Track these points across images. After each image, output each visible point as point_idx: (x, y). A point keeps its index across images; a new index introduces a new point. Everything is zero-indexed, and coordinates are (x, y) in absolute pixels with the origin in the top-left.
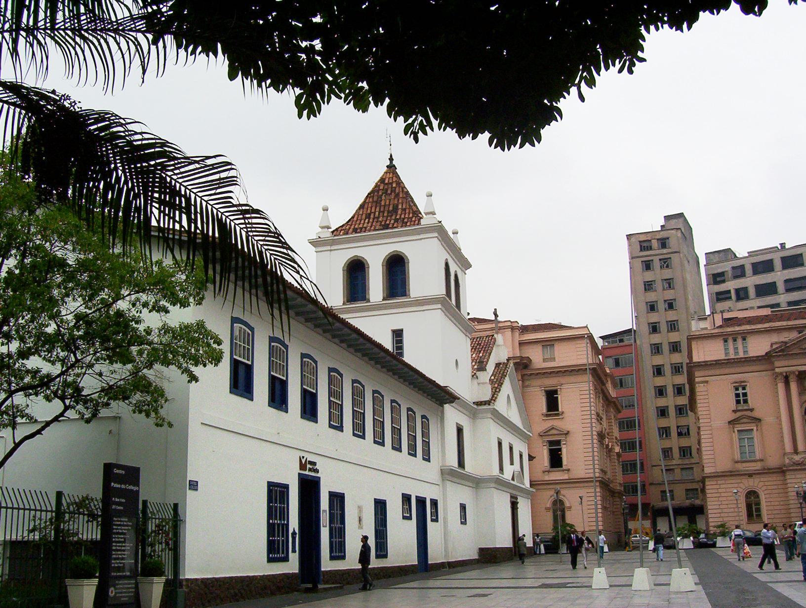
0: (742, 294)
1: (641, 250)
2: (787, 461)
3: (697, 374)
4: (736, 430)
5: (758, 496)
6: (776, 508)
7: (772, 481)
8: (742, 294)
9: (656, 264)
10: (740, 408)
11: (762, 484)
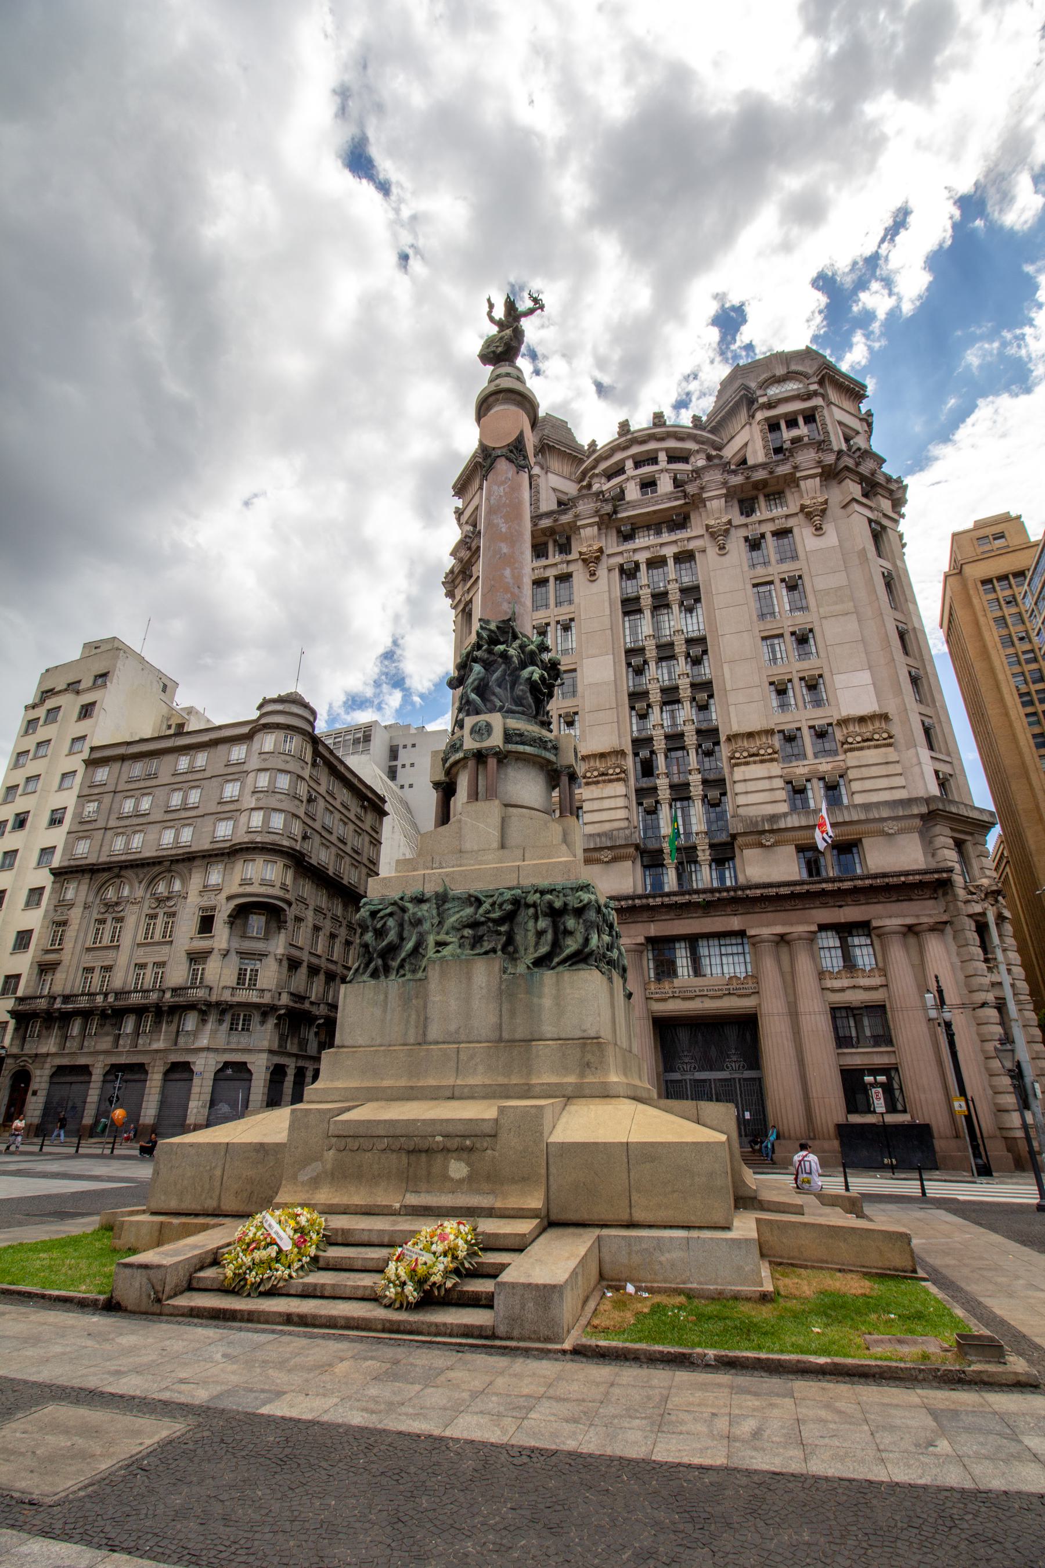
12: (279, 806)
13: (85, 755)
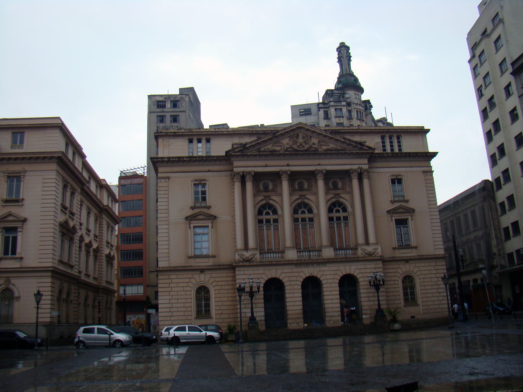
1: (158, 107)
2: (237, 257)
3: (160, 169)
4: (192, 226)
6: (224, 303)
7: (224, 276)
9: (168, 119)
10: (198, 205)
11: (213, 279)
13: (510, 70)
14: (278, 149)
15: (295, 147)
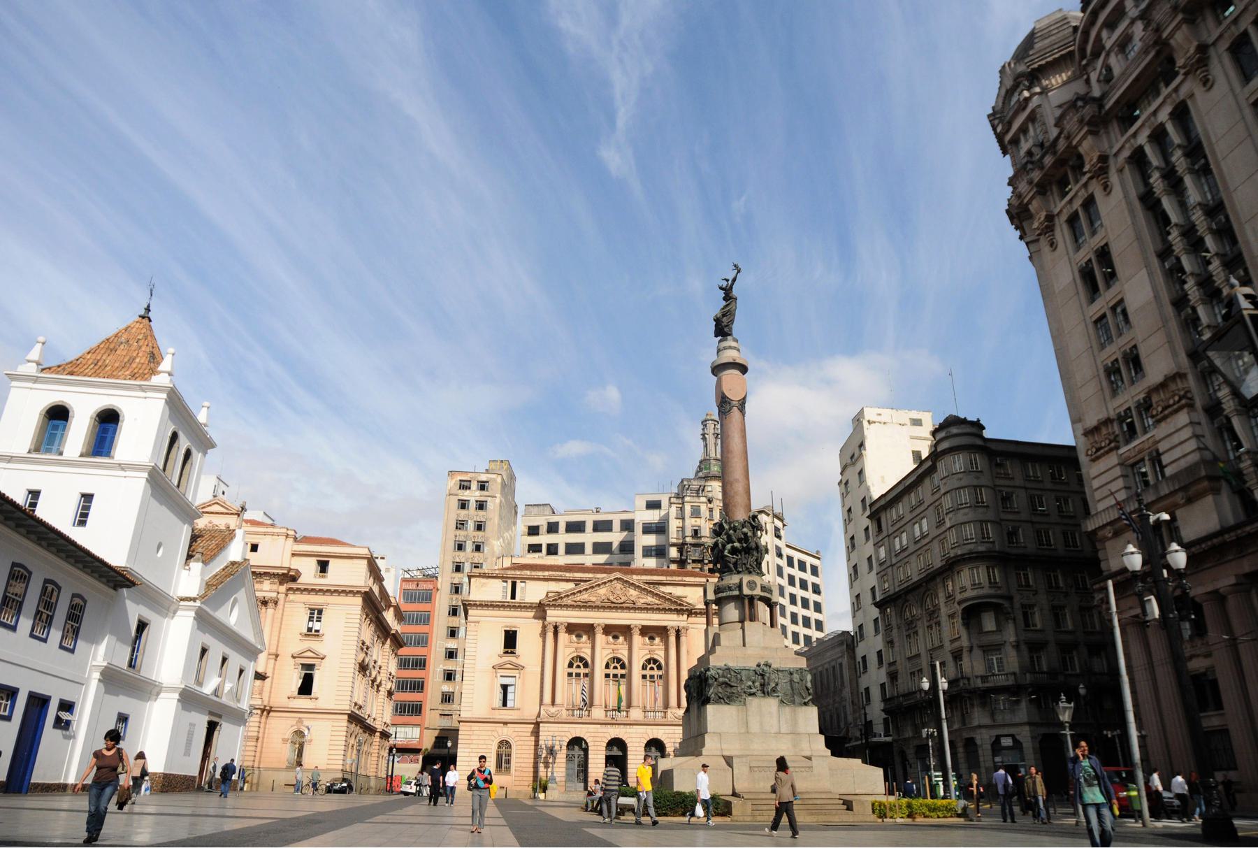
0: (552, 549)
3: (470, 612)
5: (510, 747)
8: (552, 549)
12: (965, 519)
14: (594, 599)
15: (611, 598)
